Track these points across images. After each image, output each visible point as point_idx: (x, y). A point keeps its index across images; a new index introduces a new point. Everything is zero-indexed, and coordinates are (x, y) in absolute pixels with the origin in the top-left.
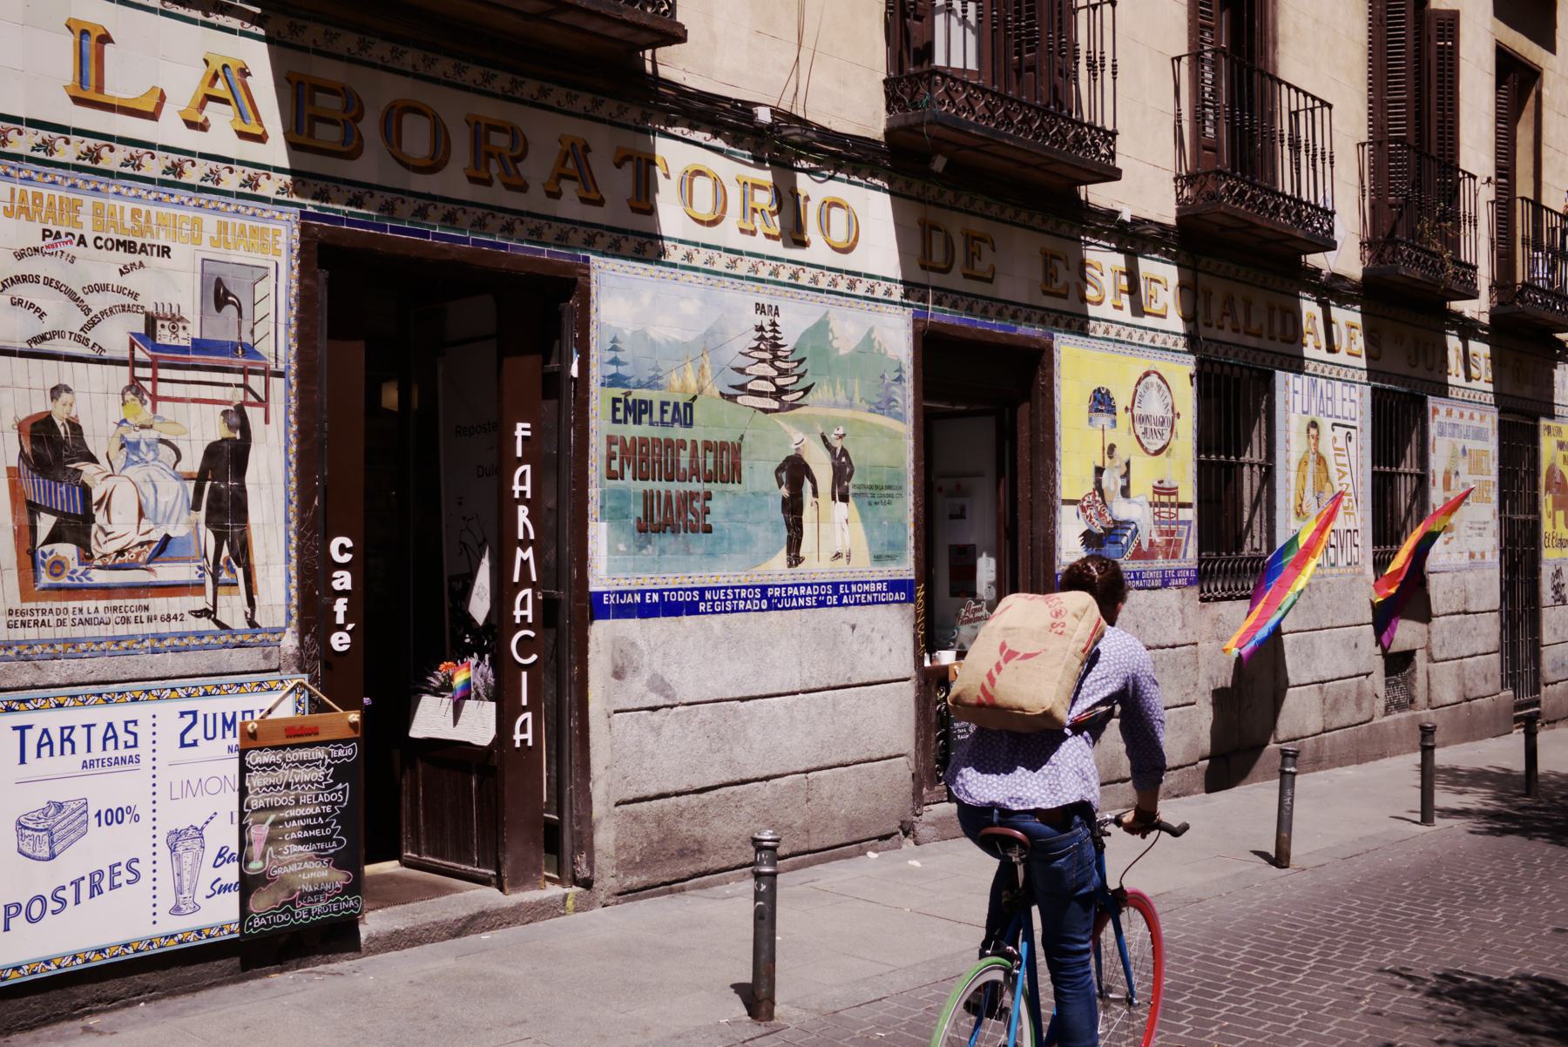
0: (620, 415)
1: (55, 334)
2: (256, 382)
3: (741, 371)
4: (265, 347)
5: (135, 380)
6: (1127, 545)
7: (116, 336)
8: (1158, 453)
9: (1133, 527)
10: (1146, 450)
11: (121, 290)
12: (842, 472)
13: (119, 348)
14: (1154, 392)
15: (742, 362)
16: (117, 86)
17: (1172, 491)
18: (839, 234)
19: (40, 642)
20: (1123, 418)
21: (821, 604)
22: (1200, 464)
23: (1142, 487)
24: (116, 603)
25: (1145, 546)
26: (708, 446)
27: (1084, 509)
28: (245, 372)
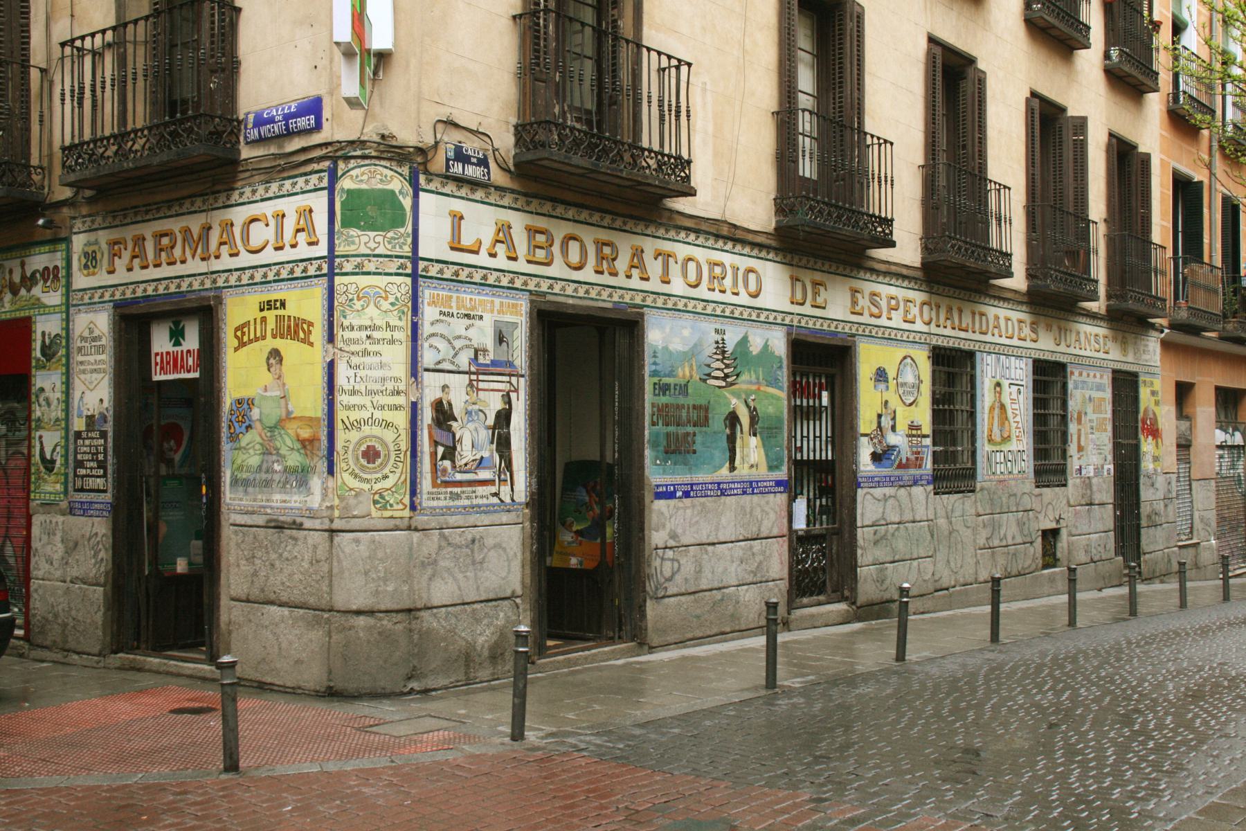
0: (657, 392)
1: (444, 360)
2: (514, 380)
3: (709, 366)
4: (517, 363)
5: (471, 381)
6: (895, 460)
7: (464, 360)
8: (911, 405)
10: (904, 403)
11: (466, 338)
12: (754, 419)
13: (465, 367)
14: (909, 368)
15: (708, 361)
16: (466, 241)
17: (918, 428)
18: (753, 287)
19: (438, 507)
20: (892, 383)
21: (744, 493)
22: (934, 411)
23: (902, 426)
24: (465, 489)
25: (904, 461)
26: (694, 407)
27: (872, 439)
28: (510, 375)
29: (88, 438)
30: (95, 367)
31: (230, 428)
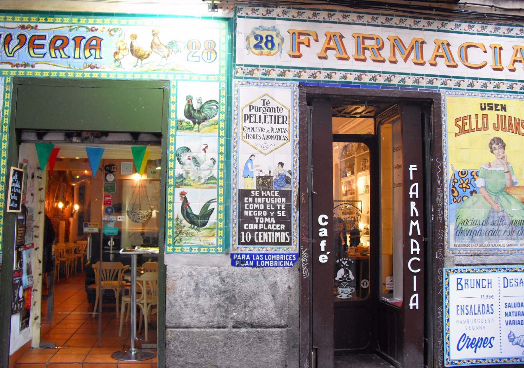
29: (260, 196)
30: (272, 134)
31: (453, 192)
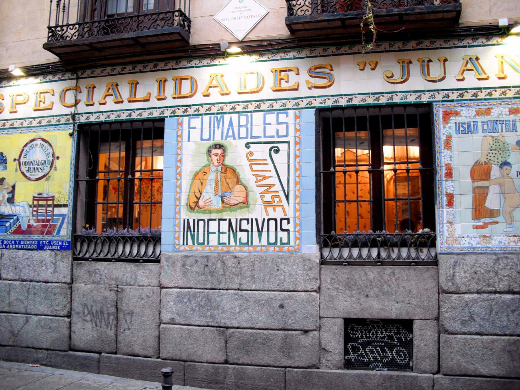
9: (15, 218)
10: (29, 179)
